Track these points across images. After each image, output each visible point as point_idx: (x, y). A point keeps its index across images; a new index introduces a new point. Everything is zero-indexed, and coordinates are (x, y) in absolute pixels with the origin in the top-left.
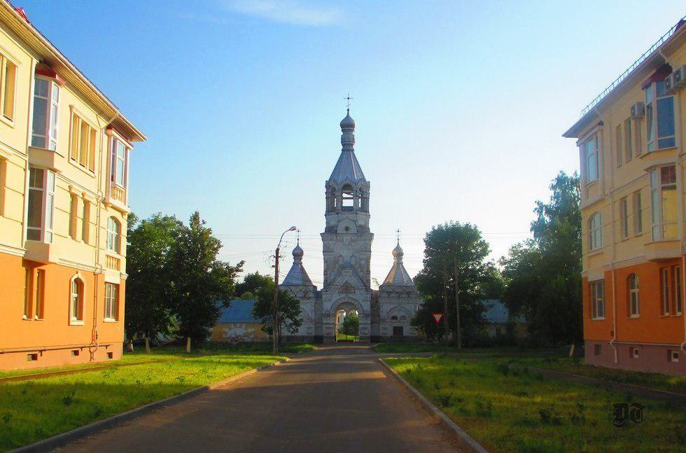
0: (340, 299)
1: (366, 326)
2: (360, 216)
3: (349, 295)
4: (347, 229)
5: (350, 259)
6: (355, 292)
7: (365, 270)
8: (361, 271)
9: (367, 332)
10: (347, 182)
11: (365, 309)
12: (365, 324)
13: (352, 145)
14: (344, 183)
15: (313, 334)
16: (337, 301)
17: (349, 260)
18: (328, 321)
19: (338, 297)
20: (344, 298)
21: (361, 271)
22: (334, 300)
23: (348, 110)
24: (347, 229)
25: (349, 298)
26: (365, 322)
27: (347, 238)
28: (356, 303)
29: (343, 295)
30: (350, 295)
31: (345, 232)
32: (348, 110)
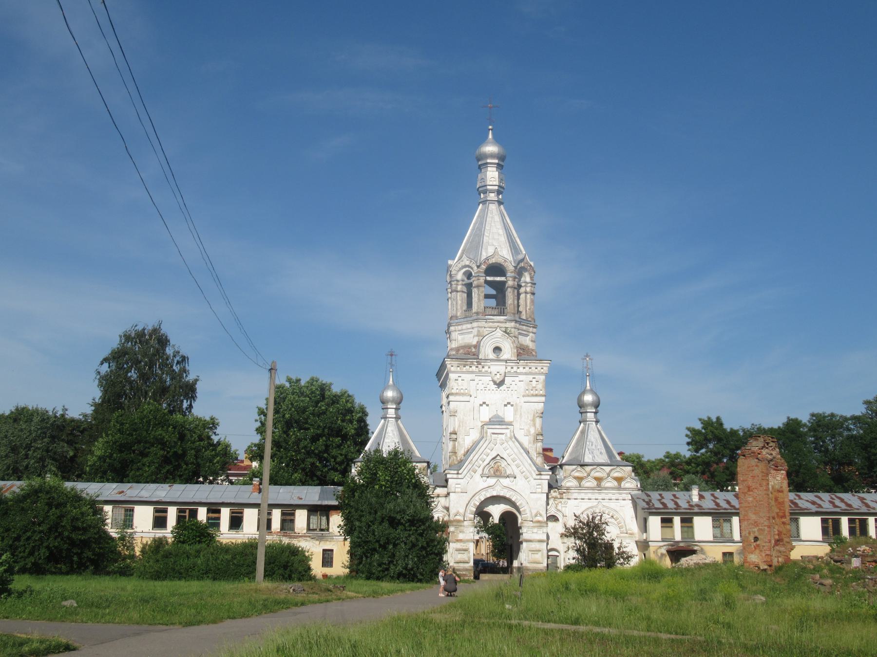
4: (497, 349)
24: (497, 349)
27: (497, 369)
29: (492, 481)
30: (505, 482)
31: (492, 356)
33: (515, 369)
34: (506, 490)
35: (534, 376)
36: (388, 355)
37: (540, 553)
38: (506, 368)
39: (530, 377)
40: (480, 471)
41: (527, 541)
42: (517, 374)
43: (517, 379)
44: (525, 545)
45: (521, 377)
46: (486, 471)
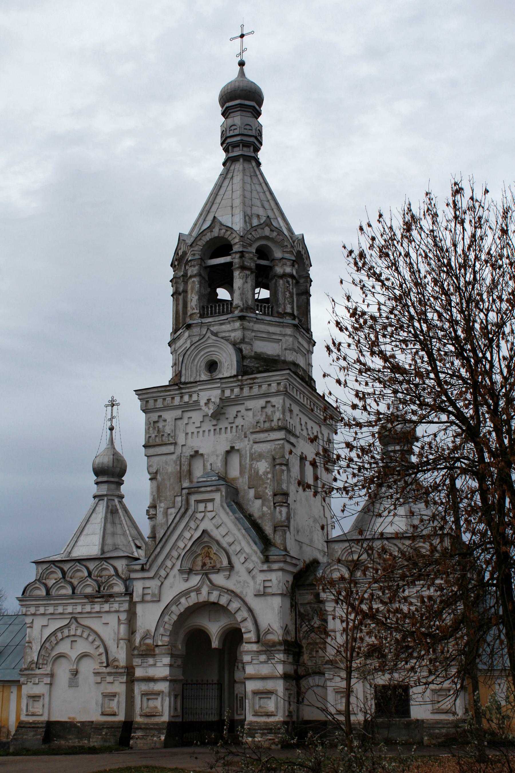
0: (186, 593)
1: (269, 685)
2: (257, 327)
3: (213, 577)
5: (226, 462)
6: (231, 567)
7: (269, 493)
8: (257, 497)
9: (270, 705)
10: (216, 232)
11: (263, 625)
12: (264, 678)
13: (257, 150)
14: (208, 237)
15: (121, 717)
16: (176, 601)
17: (219, 465)
18: (152, 672)
19: (184, 586)
20: (198, 590)
21: (257, 497)
22: (167, 597)
23: (242, 64)
25: (214, 586)
26: (265, 670)
28: (235, 605)
29: (195, 580)
31: (204, 377)
32: (242, 64)
33: (237, 390)
34: (216, 593)
35: (268, 399)
36: (106, 406)
37: (273, 697)
38: (223, 391)
39: (262, 402)
40: (178, 567)
41: (251, 678)
42: (237, 401)
43: (241, 408)
44: (251, 686)
45: (250, 404)
46: (188, 565)
